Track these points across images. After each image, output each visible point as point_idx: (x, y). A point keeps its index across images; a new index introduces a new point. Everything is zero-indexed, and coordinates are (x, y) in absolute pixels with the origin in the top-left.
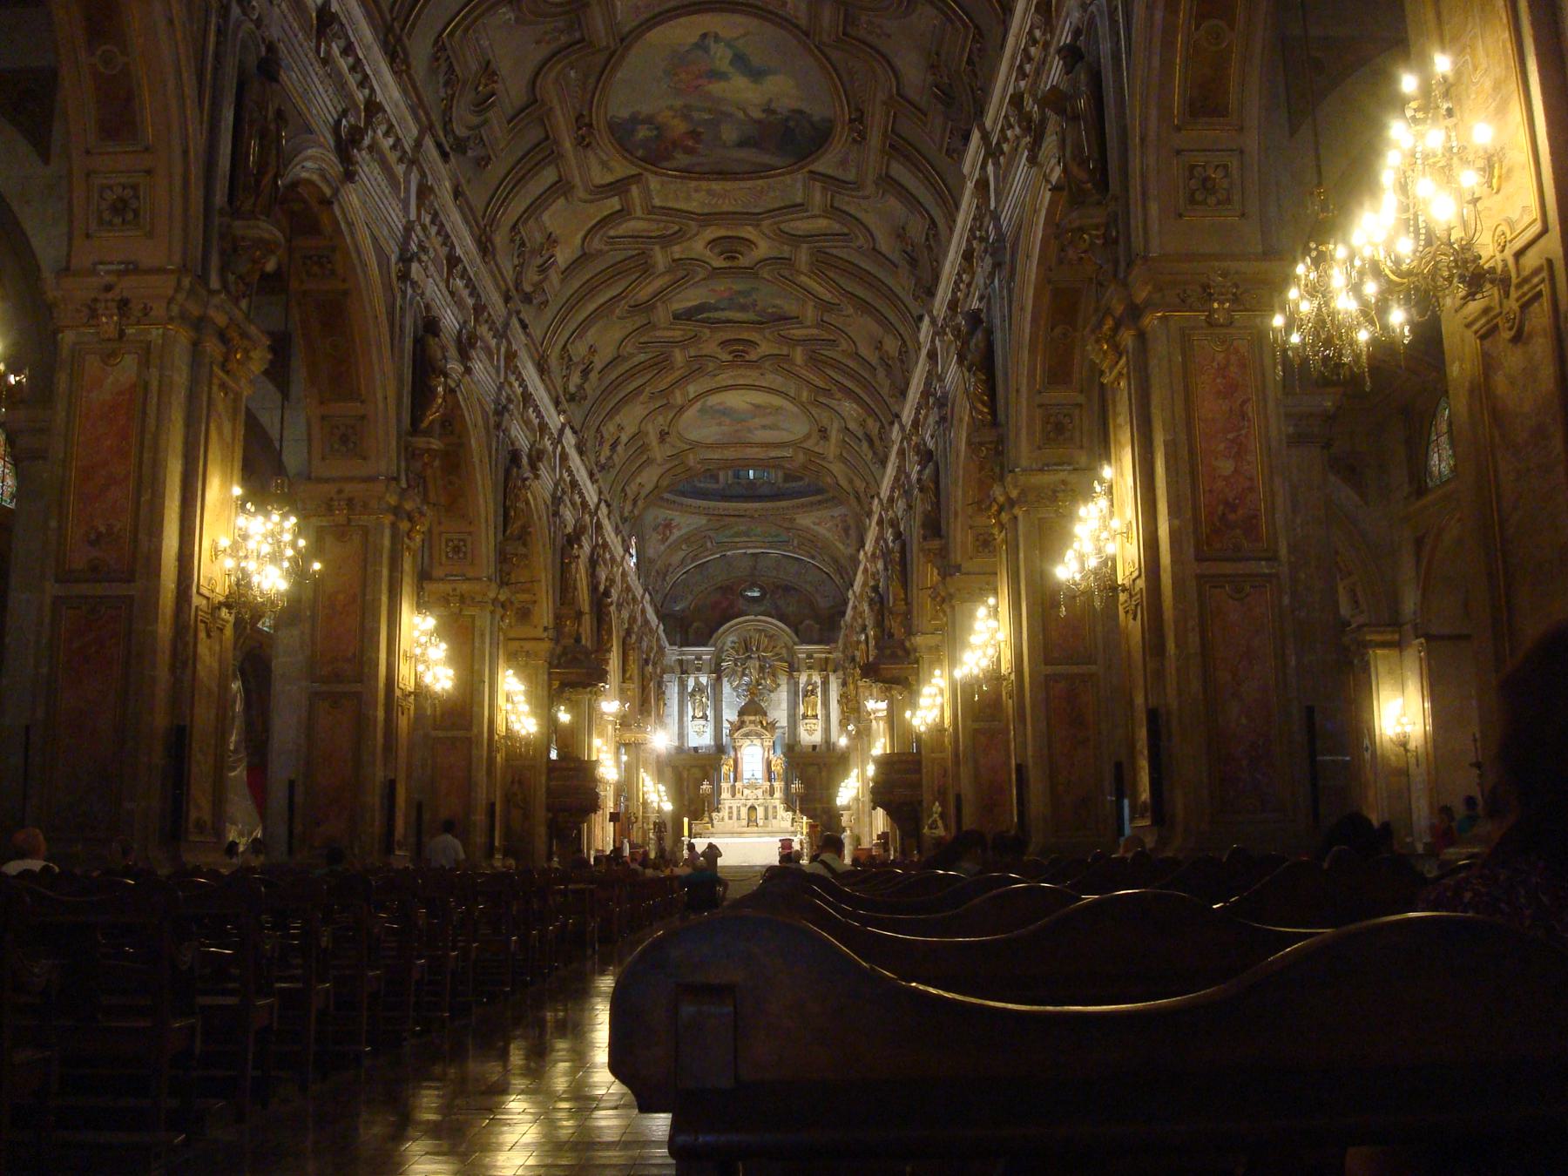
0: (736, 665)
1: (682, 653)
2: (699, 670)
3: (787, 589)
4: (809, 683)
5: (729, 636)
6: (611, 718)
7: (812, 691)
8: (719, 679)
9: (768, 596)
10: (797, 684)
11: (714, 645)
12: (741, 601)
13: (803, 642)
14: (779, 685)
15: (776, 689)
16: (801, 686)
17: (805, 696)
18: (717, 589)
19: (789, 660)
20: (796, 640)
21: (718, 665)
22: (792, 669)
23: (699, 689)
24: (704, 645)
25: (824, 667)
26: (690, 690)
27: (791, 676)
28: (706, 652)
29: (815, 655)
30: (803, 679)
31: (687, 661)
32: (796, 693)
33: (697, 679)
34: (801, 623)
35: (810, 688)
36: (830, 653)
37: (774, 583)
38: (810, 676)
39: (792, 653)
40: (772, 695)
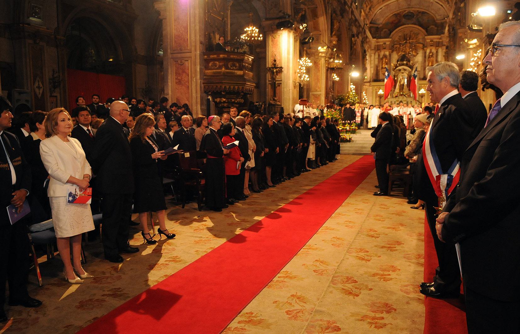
0: (400, 46)
1: (377, 42)
2: (385, 48)
3: (423, 13)
4: (430, 52)
5: (397, 33)
6: (323, 55)
7: (432, 55)
8: (393, 51)
9: (415, 16)
10: (425, 53)
11: (391, 38)
12: (404, 19)
13: (429, 35)
14: (418, 54)
15: (416, 55)
16: (427, 54)
17: (429, 58)
18: (394, 14)
19: (423, 43)
20: (426, 34)
21: (393, 46)
22: (424, 47)
23: (385, 56)
24: (388, 38)
25: (438, 45)
26: (381, 57)
27: (423, 49)
28: (388, 41)
29: (435, 40)
30: (428, 51)
31: (380, 45)
32: (425, 57)
33: (384, 52)
34: (428, 27)
35: (431, 54)
36: (440, 39)
37: (418, 11)
38: (431, 50)
39: (424, 39)
40: (414, 58)
